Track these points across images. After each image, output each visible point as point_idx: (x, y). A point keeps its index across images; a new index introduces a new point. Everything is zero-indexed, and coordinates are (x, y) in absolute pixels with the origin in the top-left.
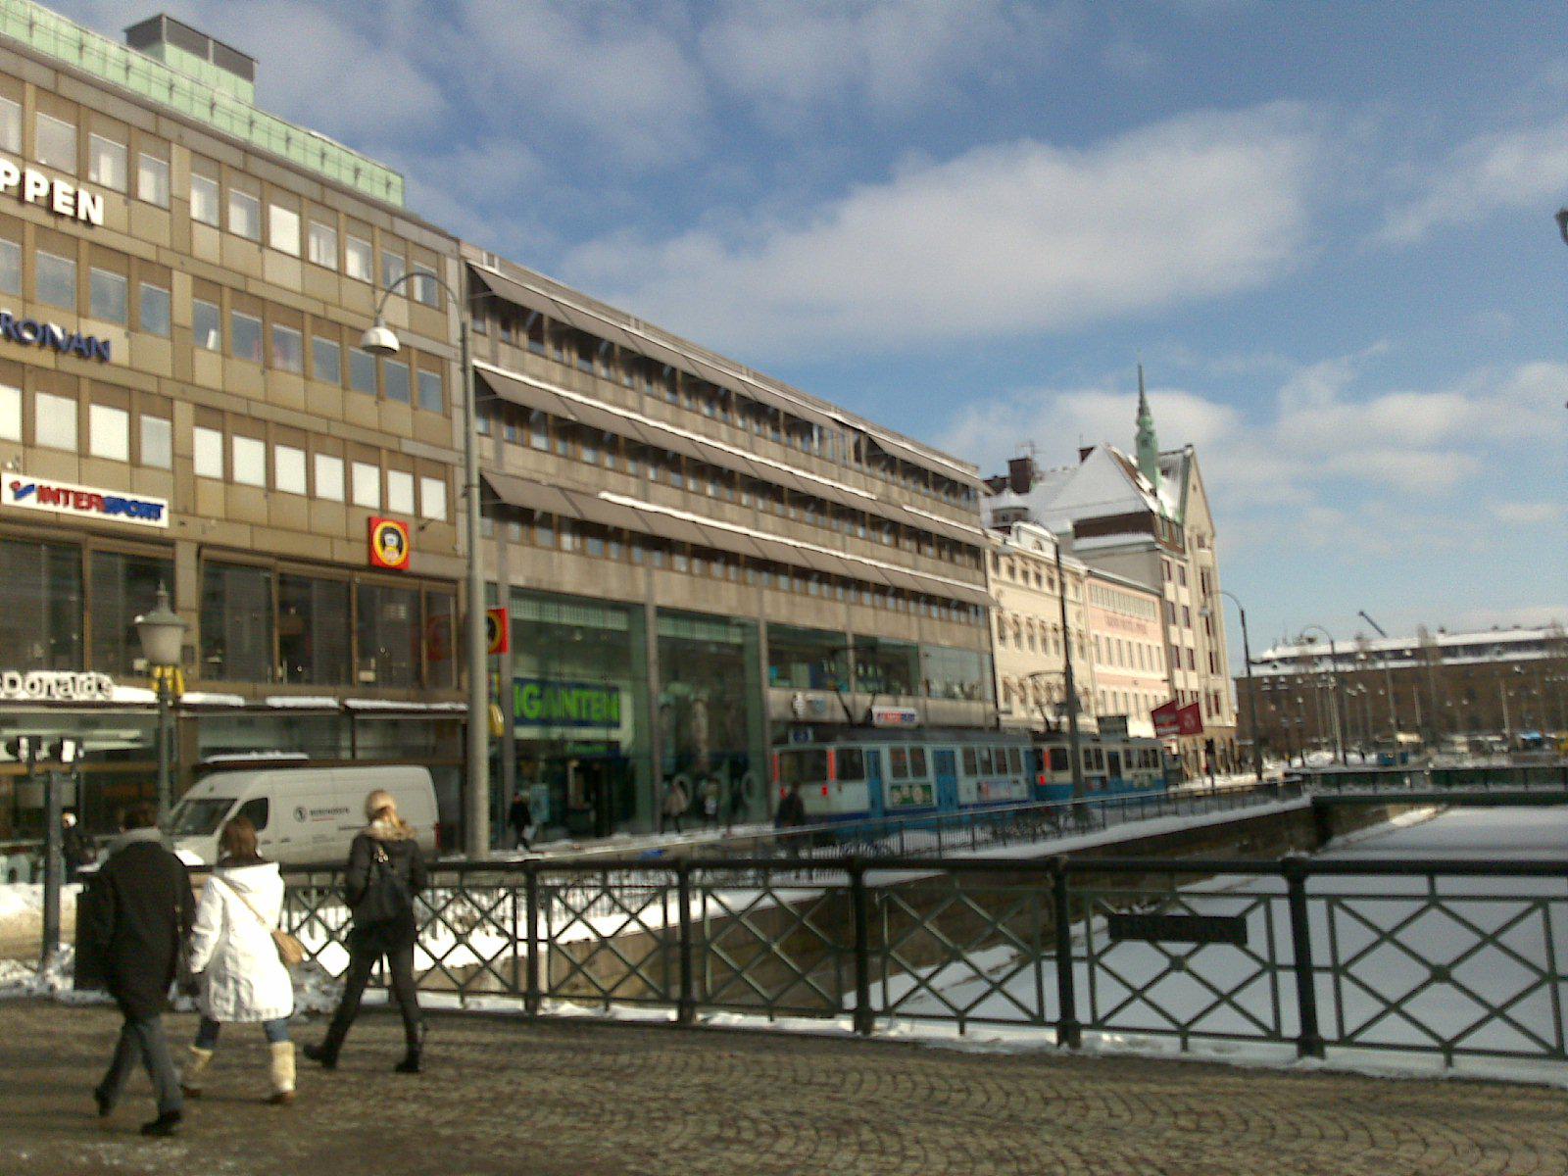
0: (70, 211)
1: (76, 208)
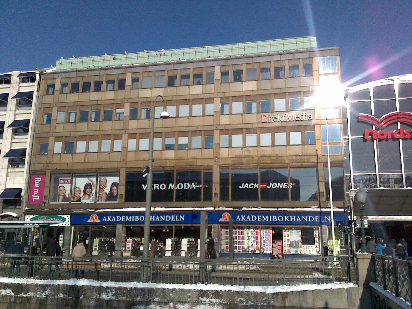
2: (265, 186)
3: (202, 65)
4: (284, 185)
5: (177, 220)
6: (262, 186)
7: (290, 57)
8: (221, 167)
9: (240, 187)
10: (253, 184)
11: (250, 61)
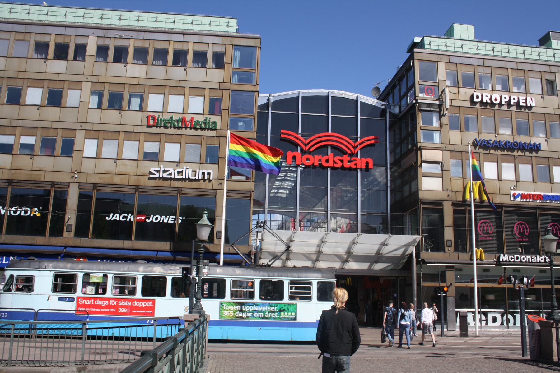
0: (525, 105)
1: (526, 103)
2: (143, 218)
3: (69, 31)
4: (170, 219)
5: (4, 262)
6: (138, 218)
7: (196, 38)
8: (80, 185)
9: (107, 218)
10: (126, 215)
11: (141, 35)
